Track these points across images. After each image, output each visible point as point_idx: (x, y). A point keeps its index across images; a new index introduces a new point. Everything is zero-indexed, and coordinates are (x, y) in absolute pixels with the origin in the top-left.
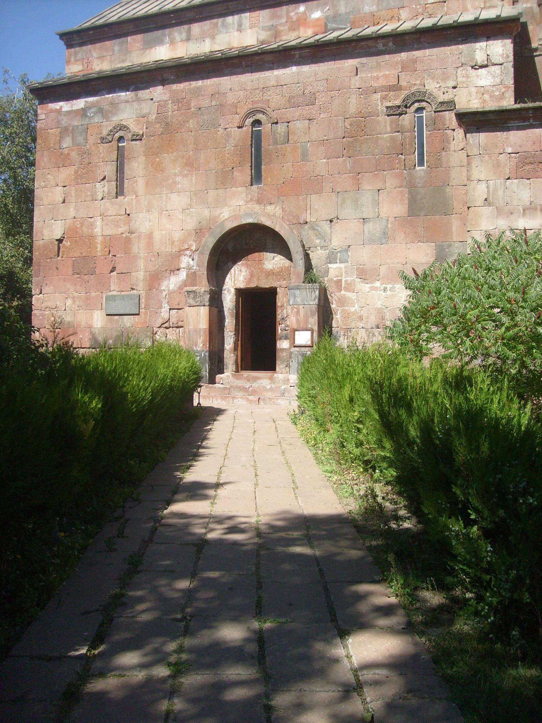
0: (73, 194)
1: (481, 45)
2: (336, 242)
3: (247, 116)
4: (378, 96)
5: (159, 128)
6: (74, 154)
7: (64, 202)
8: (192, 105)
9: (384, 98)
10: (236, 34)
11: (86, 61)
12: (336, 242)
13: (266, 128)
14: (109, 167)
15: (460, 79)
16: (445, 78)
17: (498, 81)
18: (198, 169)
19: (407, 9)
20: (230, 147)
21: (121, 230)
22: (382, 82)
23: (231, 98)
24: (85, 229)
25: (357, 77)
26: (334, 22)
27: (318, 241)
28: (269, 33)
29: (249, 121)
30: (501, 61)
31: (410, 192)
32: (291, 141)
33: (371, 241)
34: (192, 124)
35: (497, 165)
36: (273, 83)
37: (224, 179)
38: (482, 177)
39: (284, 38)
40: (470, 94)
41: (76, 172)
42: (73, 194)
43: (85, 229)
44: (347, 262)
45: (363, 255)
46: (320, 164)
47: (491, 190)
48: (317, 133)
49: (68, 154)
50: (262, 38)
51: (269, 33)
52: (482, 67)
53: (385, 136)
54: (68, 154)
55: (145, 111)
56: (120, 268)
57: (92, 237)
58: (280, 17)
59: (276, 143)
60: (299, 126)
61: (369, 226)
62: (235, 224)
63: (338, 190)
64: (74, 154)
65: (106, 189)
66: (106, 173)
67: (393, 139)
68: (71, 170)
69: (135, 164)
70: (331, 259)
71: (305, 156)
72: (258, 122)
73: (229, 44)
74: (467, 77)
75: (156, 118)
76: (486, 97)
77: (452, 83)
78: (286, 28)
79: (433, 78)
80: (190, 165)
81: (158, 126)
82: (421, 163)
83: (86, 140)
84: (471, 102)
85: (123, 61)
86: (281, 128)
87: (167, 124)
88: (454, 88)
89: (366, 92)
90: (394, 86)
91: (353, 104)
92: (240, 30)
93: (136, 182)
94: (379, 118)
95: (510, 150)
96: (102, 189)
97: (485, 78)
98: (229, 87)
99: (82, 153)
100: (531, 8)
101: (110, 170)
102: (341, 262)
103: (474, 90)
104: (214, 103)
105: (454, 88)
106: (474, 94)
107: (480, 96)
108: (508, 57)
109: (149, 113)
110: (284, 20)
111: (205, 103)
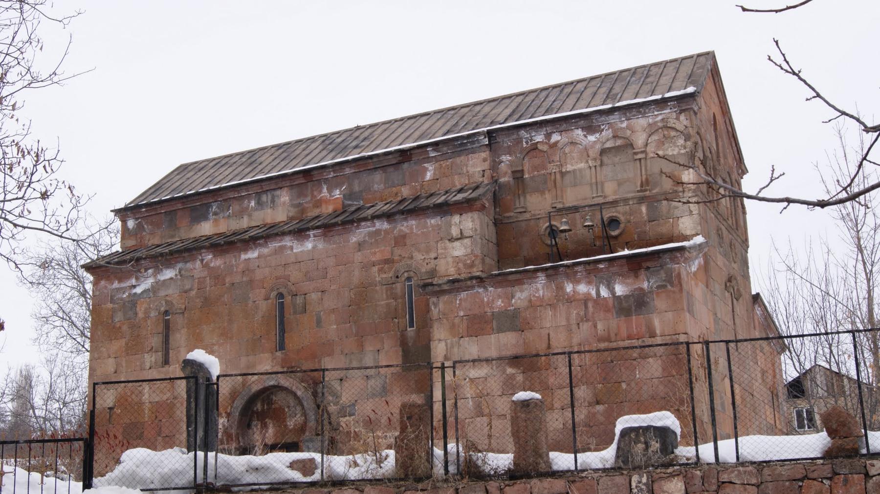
0: (124, 365)
1: (456, 219)
2: (345, 399)
3: (272, 290)
4: (375, 269)
5: (198, 302)
6: (125, 328)
7: (116, 372)
8: (227, 280)
9: (381, 271)
10: (269, 211)
11: (139, 236)
12: (345, 399)
13: (288, 299)
14: (156, 339)
15: (440, 251)
16: (428, 251)
17: (469, 250)
18: (231, 338)
19: (408, 187)
20: (258, 317)
21: (165, 398)
22: (378, 257)
23: (259, 275)
24: (134, 396)
25: (359, 253)
26: (350, 199)
27: (331, 398)
28: (296, 209)
29: (273, 294)
30: (471, 233)
31: (403, 351)
32: (308, 311)
33: (374, 395)
34: (226, 298)
35: (453, 326)
36: (293, 260)
37: (254, 346)
38: (442, 337)
39: (309, 214)
40: (447, 262)
41: (127, 344)
42: (124, 365)
43: (134, 396)
44: (354, 414)
45: (366, 408)
46: (332, 329)
47: (449, 346)
48: (330, 302)
49: (120, 327)
50: (291, 214)
51: (296, 209)
52: (458, 239)
53: (382, 303)
54: (120, 327)
55: (187, 287)
56: (166, 431)
57: (140, 404)
58: (306, 196)
59: (295, 313)
60: (314, 296)
61: (372, 382)
62: (260, 387)
63: (346, 352)
64: (125, 328)
65: (153, 359)
66: (153, 345)
67: (388, 305)
68: (123, 342)
69: (178, 336)
70: (343, 413)
71: (319, 322)
72: (281, 296)
73: (263, 220)
74: (445, 249)
75: (197, 294)
76: (461, 265)
77: (433, 255)
78: (311, 205)
79: (419, 251)
80: (225, 334)
81: (198, 301)
82: (412, 326)
83: (136, 314)
84: (448, 269)
85: (173, 236)
86: (299, 300)
87: (206, 298)
88: (436, 258)
89: (366, 266)
90: (388, 260)
91: (357, 275)
92: (273, 208)
93: (179, 352)
94: (377, 288)
95: (462, 314)
96: (149, 359)
97: (459, 250)
98: (257, 264)
99: (132, 327)
100: (509, 182)
101: (156, 341)
102: (350, 415)
103: (450, 260)
104: (244, 279)
105: (436, 258)
106: (451, 263)
107: (455, 264)
108: (476, 230)
109: (191, 289)
110: (309, 198)
111: (237, 279)
